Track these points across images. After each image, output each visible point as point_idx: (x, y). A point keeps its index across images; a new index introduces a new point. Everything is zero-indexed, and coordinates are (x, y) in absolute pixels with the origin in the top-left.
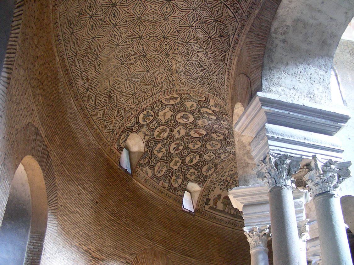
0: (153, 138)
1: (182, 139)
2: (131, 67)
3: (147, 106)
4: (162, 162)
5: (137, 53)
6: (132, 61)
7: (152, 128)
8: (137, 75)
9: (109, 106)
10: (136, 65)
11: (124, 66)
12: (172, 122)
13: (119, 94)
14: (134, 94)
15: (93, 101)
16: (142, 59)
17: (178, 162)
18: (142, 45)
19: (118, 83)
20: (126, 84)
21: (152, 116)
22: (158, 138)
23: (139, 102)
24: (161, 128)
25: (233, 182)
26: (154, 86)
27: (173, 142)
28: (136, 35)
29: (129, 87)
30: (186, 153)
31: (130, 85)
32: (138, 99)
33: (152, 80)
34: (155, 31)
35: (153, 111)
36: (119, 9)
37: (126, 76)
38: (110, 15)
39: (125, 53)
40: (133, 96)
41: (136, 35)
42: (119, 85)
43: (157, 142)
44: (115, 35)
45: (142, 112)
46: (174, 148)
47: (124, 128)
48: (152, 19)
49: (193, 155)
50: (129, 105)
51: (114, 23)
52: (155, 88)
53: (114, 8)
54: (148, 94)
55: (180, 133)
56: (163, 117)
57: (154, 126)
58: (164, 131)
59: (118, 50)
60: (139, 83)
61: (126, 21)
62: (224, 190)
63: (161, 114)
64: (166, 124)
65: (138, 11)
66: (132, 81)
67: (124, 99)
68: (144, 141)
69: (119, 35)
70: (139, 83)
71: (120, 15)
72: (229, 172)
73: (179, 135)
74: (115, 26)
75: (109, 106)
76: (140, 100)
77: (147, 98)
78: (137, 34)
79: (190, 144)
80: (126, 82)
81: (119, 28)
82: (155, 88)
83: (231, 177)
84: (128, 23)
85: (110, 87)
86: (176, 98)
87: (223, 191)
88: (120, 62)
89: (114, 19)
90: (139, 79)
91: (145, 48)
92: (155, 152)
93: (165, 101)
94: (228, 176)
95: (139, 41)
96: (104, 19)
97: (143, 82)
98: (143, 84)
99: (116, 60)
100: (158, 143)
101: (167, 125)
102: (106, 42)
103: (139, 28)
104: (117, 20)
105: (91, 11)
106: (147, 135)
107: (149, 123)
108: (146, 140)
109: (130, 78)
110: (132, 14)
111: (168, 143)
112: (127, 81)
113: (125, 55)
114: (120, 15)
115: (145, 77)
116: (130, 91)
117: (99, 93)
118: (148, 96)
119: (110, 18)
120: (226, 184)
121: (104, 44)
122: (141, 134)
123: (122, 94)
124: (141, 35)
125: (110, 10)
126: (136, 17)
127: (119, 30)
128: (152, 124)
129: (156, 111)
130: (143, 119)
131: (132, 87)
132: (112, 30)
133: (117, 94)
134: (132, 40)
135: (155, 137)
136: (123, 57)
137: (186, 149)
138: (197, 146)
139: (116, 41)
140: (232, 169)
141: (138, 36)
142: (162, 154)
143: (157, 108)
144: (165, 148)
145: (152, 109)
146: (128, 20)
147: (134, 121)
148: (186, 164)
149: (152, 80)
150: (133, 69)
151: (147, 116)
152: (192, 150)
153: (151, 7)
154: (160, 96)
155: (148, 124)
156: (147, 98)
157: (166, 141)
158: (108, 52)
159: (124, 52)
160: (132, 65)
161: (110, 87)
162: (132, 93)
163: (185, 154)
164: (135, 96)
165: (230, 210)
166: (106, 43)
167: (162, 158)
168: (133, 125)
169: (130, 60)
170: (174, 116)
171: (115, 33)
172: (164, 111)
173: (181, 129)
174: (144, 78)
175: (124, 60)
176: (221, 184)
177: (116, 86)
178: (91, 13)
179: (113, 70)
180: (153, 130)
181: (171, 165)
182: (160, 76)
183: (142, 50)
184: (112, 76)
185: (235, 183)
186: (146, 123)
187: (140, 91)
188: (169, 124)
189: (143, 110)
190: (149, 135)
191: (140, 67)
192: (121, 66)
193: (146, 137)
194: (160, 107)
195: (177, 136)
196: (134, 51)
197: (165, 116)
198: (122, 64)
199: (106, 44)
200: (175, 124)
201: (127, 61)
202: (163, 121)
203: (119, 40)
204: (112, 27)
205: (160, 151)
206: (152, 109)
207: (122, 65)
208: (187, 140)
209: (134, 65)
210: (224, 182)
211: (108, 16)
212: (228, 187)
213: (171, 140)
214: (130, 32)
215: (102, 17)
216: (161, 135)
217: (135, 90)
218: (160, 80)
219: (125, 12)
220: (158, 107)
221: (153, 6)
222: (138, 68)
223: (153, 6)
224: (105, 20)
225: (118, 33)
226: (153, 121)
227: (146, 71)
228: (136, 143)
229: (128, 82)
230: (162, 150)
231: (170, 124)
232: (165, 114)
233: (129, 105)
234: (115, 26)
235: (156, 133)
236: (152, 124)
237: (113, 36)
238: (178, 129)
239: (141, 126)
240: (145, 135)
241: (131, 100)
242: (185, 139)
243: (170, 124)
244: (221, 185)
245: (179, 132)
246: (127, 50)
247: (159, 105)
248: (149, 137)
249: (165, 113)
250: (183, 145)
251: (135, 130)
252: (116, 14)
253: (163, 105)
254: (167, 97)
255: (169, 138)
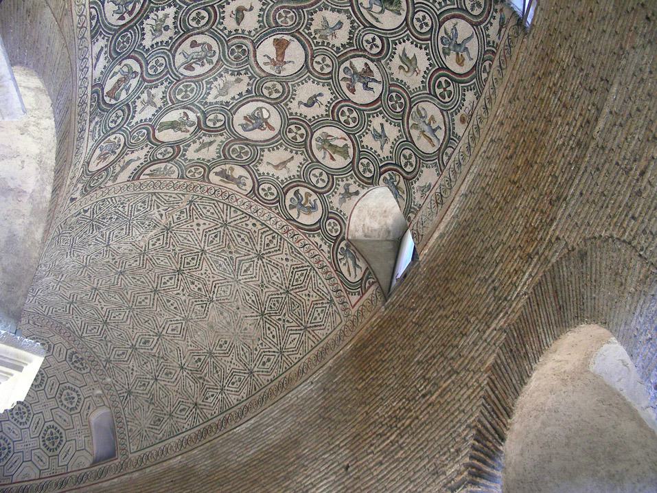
0: (353, 166)
1: (329, 79)
2: (211, 283)
3: (278, 214)
4: (411, 122)
5: (182, 284)
6: (200, 286)
7: (326, 180)
8: (220, 265)
9: (285, 315)
10: (204, 276)
11: (215, 295)
12: (290, 135)
13: (267, 290)
14: (260, 257)
15: (269, 360)
16: (188, 271)
17: (404, 58)
18: (165, 283)
19: (248, 298)
20: (245, 279)
21: (296, 193)
22: (351, 151)
23: (273, 237)
24: (319, 155)
26: (225, 225)
27: (349, 100)
28: (156, 299)
29: (249, 273)
30: (369, 37)
31: (245, 271)
32: (267, 241)
33: (216, 236)
34: (129, 284)
35: (285, 194)
36: (135, 340)
37: (231, 285)
38: (148, 349)
39: (193, 303)
40: (265, 256)
41: (156, 299)
42: (251, 294)
43: (361, 152)
44: (173, 330)
45: (294, 220)
46: (366, 87)
47: (330, 263)
48: (117, 297)
49: (369, 9)
50: (287, 259)
51: (156, 338)
52: (229, 221)
53: (137, 346)
54: (249, 227)
55: (315, 96)
56: (289, 165)
57: (321, 174)
58: (326, 142)
59: (194, 316)
60: (234, 256)
61: (146, 322)
63: (282, 174)
64: (305, 146)
65: (121, 317)
66: (236, 271)
67: (275, 274)
68: (362, 192)
69: (170, 323)
70: (234, 256)
71: (143, 335)
73: (320, 95)
74: (160, 336)
75: (285, 315)
76: (270, 237)
77: (258, 224)
78: (154, 299)
79: (337, 43)
80: (242, 282)
81: (160, 327)
82: (229, 221)
84: (147, 319)
85: (255, 314)
86: (222, 174)
88: (211, 305)
89: (151, 340)
90: (225, 259)
91: (167, 278)
92: (386, 152)
93: (245, 185)
95: (162, 292)
96: (155, 356)
97: (229, 248)
98: (232, 247)
99: (208, 313)
100: (363, 147)
101: (306, 144)
102: (186, 342)
103: (143, 300)
104: (149, 335)
105: (149, 383)
106: (347, 187)
107: (316, 192)
108: (359, 189)
109: (232, 276)
110: (132, 320)
111: (355, 114)
112: (240, 280)
113: (196, 301)
114: (143, 335)
115: (216, 251)
116: (257, 265)
117: (261, 341)
118: (254, 225)
119: (152, 347)
121: (189, 344)
122: (346, 207)
123: (265, 282)
124: (152, 294)
125: (142, 351)
126: (131, 313)
127: (163, 326)
128: (317, 182)
129: (283, 189)
130: (310, 213)
131: (247, 265)
132: (166, 338)
133: (267, 294)
134: (169, 301)
135: (349, 160)
136: (201, 303)
137: (360, 42)
138: (333, 18)
139: (179, 325)
141: (157, 296)
142: (387, 126)
143: (274, 190)
144: (371, 119)
145: (279, 200)
146: (143, 321)
147: (319, 235)
148: (406, 19)
149: (216, 236)
150: (213, 277)
151: (300, 205)
152: (352, 22)
153: (102, 308)
154: (242, 202)
155: (320, 193)
156: (258, 224)
157: (352, 125)
158: (199, 333)
159: (192, 305)
160: (208, 282)
161: (255, 314)
162: (260, 262)
163: (374, 39)
164: (263, 252)
166: (188, 342)
167: (399, 126)
168: (326, 237)
169: (199, 289)
170: (271, 144)
171: (169, 331)
172: (272, 171)
173: (300, 103)
174: (219, 251)
175: (203, 299)
177: (253, 301)
178: (152, 382)
179: (225, 314)
180: (331, 174)
181: (414, 81)
182: (198, 230)
183: (173, 280)
184: (237, 314)
186: (318, 202)
187: (250, 246)
188: (299, 139)
189: (290, 219)
190: (345, 182)
191: (204, 268)
192: (217, 300)
193: (353, 189)
194: (266, 186)
195: (327, 96)
196: (183, 290)
197: (284, 164)
198: (212, 301)
199: (189, 340)
200: (292, 127)
201: (204, 293)
202: (299, 158)
203: (177, 320)
204: (163, 340)
205: (380, 136)
206: (279, 200)
207: (215, 299)
208: (328, 61)
209: (207, 279)
211: (150, 351)
213: (345, 109)
214: (158, 310)
215: (154, 360)
216: (340, 143)
217: (251, 256)
218: (205, 224)
219: (135, 331)
220: (269, 189)
221: (99, 307)
222: (206, 270)
223: (99, 307)
224: (157, 355)
225: (167, 325)
226: (308, 184)
227: (204, 256)
228: (374, 210)
229: (240, 278)
230: (379, 131)
231: (298, 137)
232: (279, 164)
233: (287, 259)
234: (159, 335)
235: (340, 162)
236: (317, 182)
237: (175, 332)
238: (304, 110)
239: (328, 214)
240: (348, 194)
241: (274, 258)
242: (327, 70)
243: (298, 137)
245: (311, 102)
246: (187, 301)
247: (263, 189)
248: (351, 181)
249: (276, 167)
250: (347, 64)
251: (339, 227)
252: (143, 340)
253: (257, 183)
254: (235, 187)
255: (342, 119)
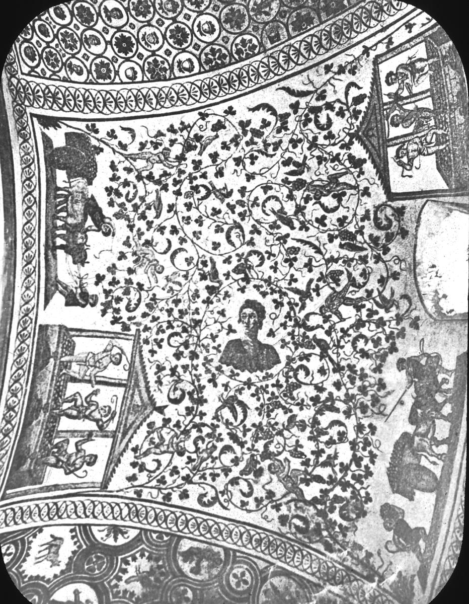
25: (324, 464)
62: (363, 493)
72: (277, 507)
83: (302, 481)
87: (368, 499)
94: (300, 497)
120: (338, 491)
140: (258, 501)
165: (439, 443)
176: (339, 521)
185: (330, 451)
210: (332, 510)
212: (348, 478)
244: (342, 516)
